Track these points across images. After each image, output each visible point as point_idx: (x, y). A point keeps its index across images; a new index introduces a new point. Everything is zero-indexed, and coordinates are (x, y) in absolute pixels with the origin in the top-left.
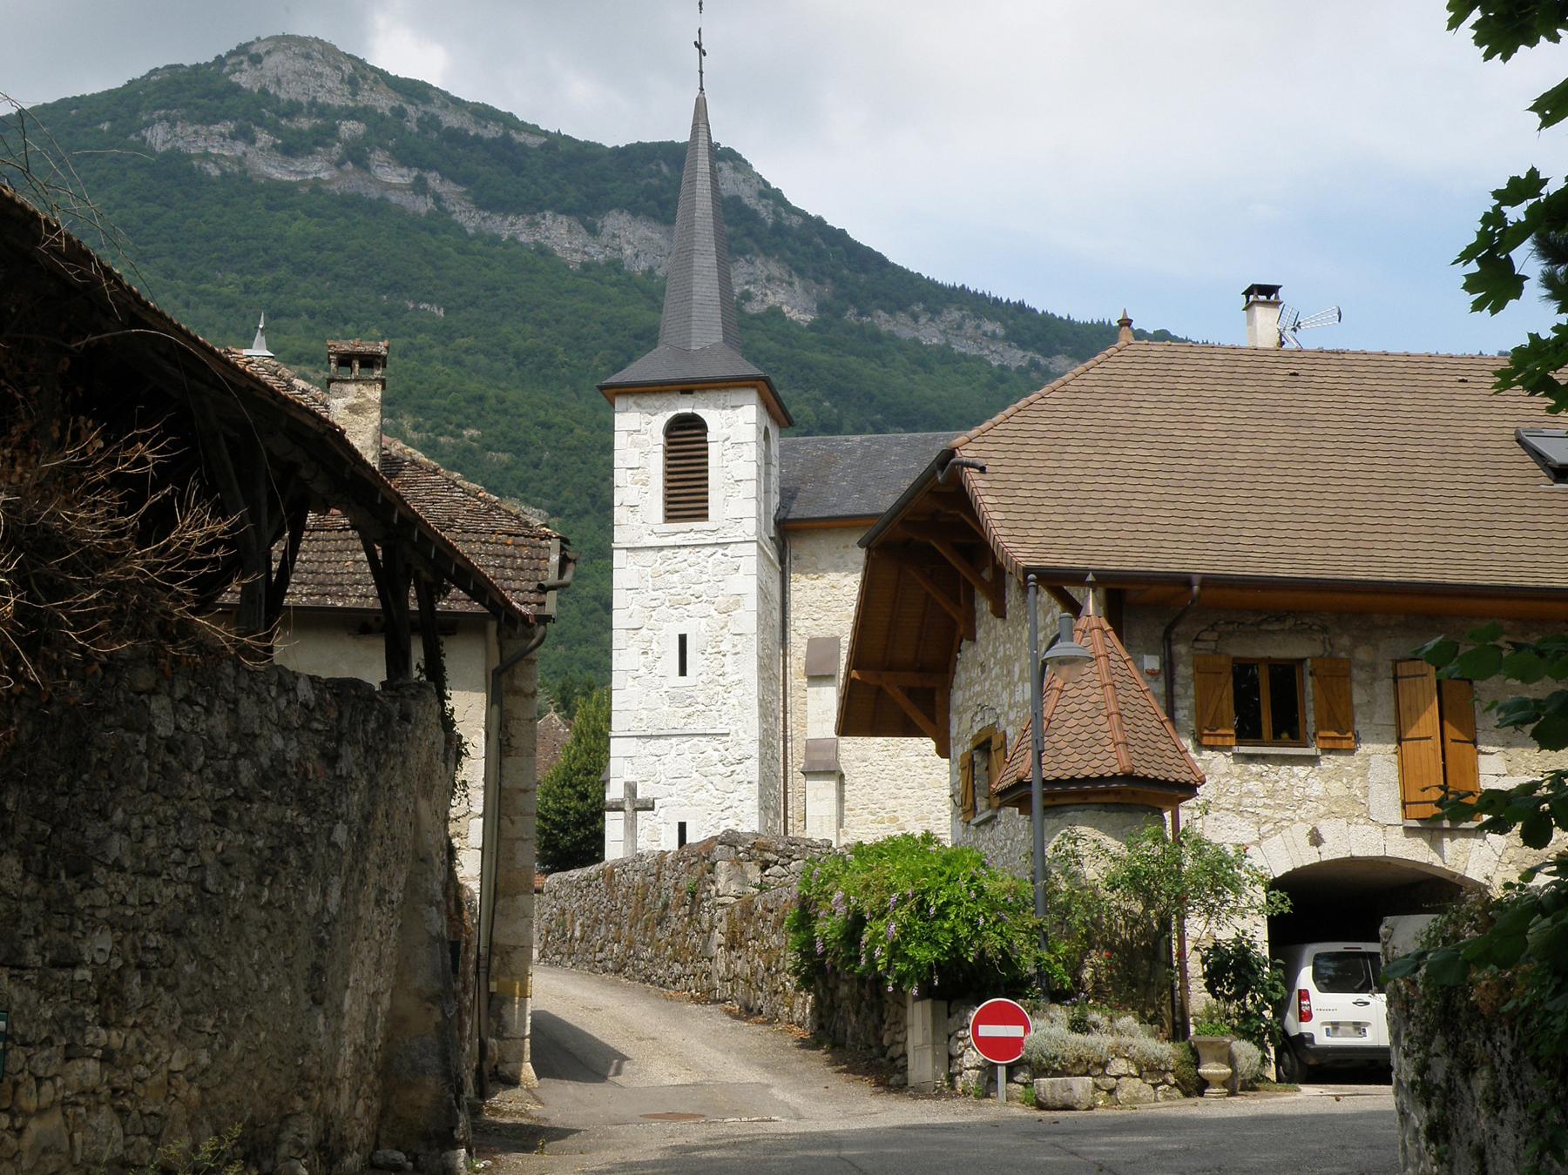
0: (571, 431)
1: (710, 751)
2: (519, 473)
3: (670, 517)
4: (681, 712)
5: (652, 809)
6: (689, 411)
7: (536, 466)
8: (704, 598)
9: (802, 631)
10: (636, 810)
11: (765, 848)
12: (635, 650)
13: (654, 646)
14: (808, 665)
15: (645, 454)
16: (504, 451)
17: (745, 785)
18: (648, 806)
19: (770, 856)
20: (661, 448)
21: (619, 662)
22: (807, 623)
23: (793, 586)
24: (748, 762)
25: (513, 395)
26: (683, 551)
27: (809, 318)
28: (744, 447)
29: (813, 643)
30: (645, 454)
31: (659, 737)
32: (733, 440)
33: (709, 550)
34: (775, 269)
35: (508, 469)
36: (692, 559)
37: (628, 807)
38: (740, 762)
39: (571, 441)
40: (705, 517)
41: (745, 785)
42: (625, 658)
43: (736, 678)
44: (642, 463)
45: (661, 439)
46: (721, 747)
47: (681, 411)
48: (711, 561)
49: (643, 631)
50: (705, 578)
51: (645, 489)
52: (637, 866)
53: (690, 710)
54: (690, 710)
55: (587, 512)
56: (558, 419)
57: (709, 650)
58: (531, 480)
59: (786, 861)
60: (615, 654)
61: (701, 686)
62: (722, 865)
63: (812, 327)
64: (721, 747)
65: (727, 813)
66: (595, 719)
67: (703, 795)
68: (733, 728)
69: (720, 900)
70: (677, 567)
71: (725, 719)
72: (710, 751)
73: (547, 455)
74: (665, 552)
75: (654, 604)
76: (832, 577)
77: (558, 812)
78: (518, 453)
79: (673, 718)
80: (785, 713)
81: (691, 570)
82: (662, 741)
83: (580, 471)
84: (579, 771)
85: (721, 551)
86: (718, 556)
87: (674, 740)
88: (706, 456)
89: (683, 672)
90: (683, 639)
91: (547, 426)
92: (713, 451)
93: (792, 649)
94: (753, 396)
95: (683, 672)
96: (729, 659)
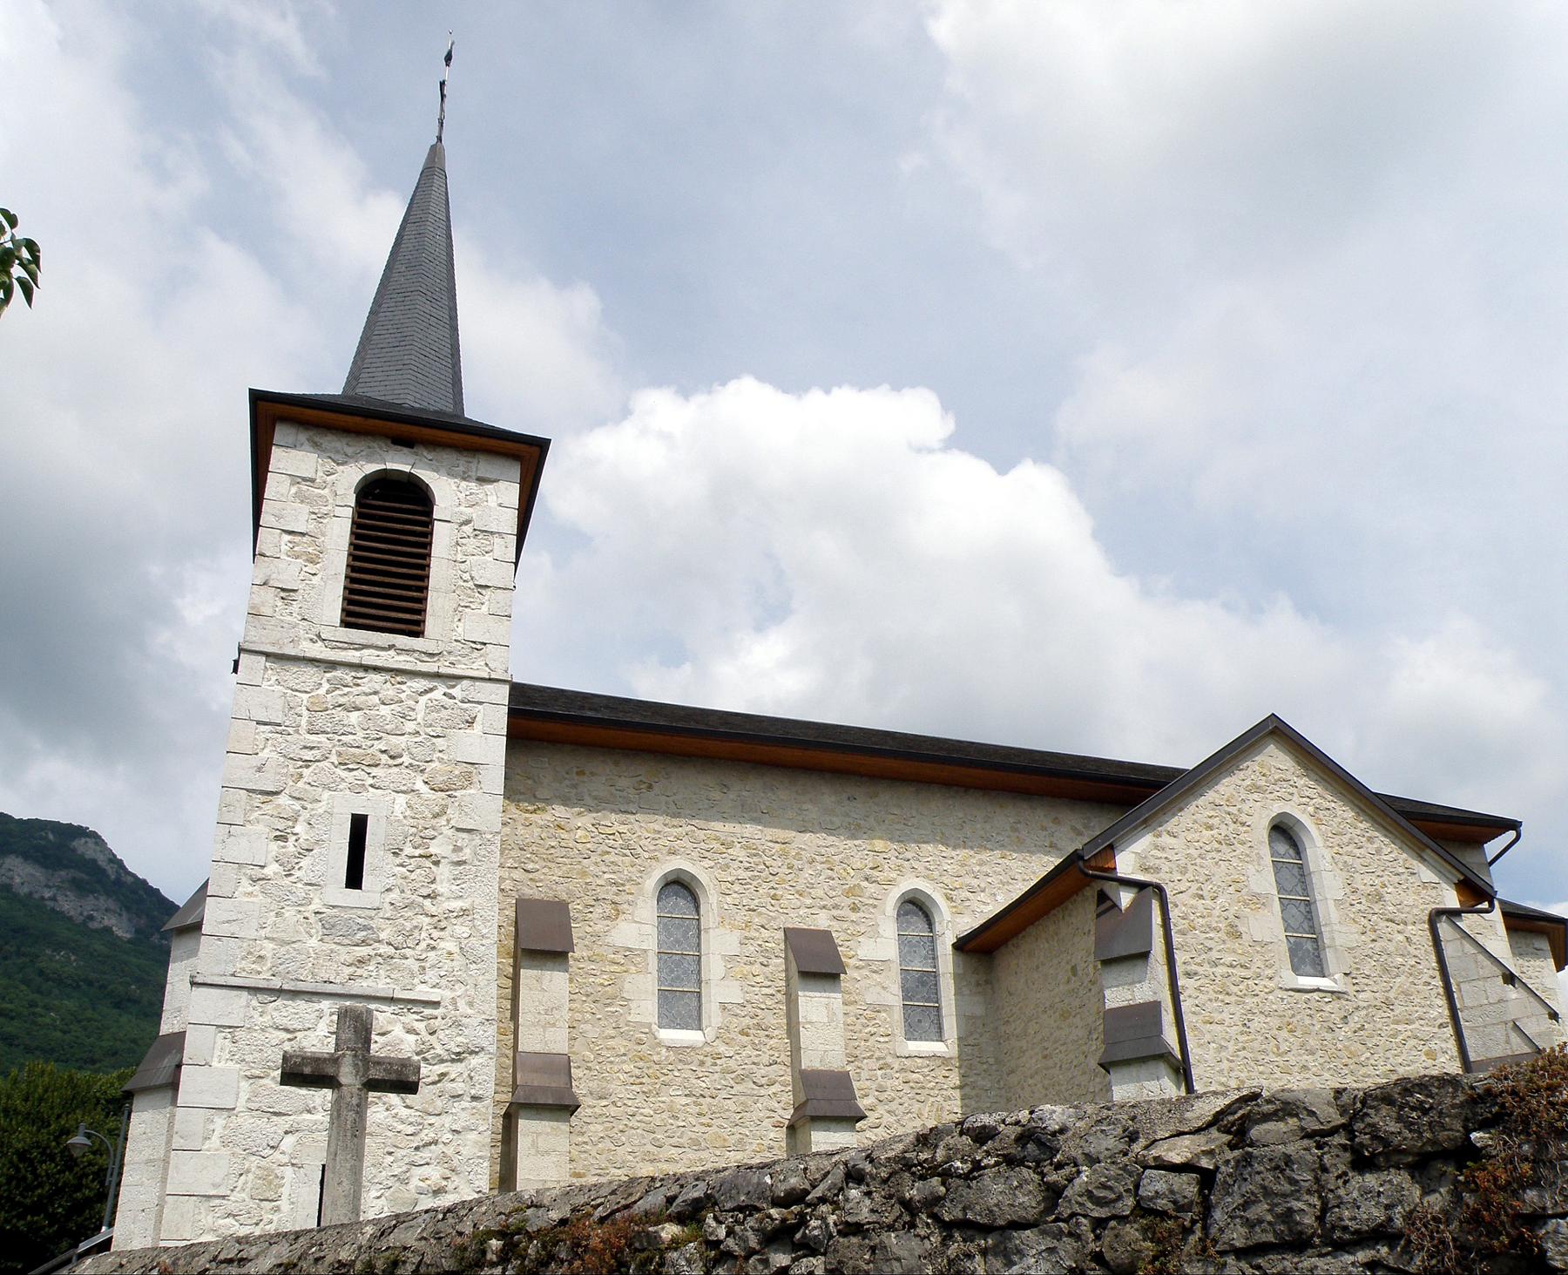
3: (346, 624)
4: (344, 954)
6: (407, 468)
8: (406, 759)
20: (349, 512)
24: (474, 1061)
26: (378, 677)
27: (128, 936)
28: (497, 540)
30: (320, 517)
31: (295, 994)
33: (421, 684)
34: (111, 904)
36: (389, 691)
37: (347, 1075)
38: (458, 1058)
40: (418, 634)
43: (457, 905)
44: (310, 527)
46: (421, 1026)
47: (390, 466)
48: (423, 702)
49: (283, 800)
50: (410, 727)
51: (311, 568)
53: (363, 951)
54: (363, 951)
57: (408, 850)
63: (129, 941)
64: (421, 1026)
65: (426, 1154)
68: (448, 994)
70: (359, 700)
71: (431, 976)
74: (338, 673)
75: (308, 755)
76: (560, 811)
81: (385, 710)
82: (301, 1004)
85: (442, 689)
86: (437, 694)
89: (354, 878)
90: (359, 826)
92: (442, 538)
94: (515, 471)
95: (354, 878)
96: (444, 871)
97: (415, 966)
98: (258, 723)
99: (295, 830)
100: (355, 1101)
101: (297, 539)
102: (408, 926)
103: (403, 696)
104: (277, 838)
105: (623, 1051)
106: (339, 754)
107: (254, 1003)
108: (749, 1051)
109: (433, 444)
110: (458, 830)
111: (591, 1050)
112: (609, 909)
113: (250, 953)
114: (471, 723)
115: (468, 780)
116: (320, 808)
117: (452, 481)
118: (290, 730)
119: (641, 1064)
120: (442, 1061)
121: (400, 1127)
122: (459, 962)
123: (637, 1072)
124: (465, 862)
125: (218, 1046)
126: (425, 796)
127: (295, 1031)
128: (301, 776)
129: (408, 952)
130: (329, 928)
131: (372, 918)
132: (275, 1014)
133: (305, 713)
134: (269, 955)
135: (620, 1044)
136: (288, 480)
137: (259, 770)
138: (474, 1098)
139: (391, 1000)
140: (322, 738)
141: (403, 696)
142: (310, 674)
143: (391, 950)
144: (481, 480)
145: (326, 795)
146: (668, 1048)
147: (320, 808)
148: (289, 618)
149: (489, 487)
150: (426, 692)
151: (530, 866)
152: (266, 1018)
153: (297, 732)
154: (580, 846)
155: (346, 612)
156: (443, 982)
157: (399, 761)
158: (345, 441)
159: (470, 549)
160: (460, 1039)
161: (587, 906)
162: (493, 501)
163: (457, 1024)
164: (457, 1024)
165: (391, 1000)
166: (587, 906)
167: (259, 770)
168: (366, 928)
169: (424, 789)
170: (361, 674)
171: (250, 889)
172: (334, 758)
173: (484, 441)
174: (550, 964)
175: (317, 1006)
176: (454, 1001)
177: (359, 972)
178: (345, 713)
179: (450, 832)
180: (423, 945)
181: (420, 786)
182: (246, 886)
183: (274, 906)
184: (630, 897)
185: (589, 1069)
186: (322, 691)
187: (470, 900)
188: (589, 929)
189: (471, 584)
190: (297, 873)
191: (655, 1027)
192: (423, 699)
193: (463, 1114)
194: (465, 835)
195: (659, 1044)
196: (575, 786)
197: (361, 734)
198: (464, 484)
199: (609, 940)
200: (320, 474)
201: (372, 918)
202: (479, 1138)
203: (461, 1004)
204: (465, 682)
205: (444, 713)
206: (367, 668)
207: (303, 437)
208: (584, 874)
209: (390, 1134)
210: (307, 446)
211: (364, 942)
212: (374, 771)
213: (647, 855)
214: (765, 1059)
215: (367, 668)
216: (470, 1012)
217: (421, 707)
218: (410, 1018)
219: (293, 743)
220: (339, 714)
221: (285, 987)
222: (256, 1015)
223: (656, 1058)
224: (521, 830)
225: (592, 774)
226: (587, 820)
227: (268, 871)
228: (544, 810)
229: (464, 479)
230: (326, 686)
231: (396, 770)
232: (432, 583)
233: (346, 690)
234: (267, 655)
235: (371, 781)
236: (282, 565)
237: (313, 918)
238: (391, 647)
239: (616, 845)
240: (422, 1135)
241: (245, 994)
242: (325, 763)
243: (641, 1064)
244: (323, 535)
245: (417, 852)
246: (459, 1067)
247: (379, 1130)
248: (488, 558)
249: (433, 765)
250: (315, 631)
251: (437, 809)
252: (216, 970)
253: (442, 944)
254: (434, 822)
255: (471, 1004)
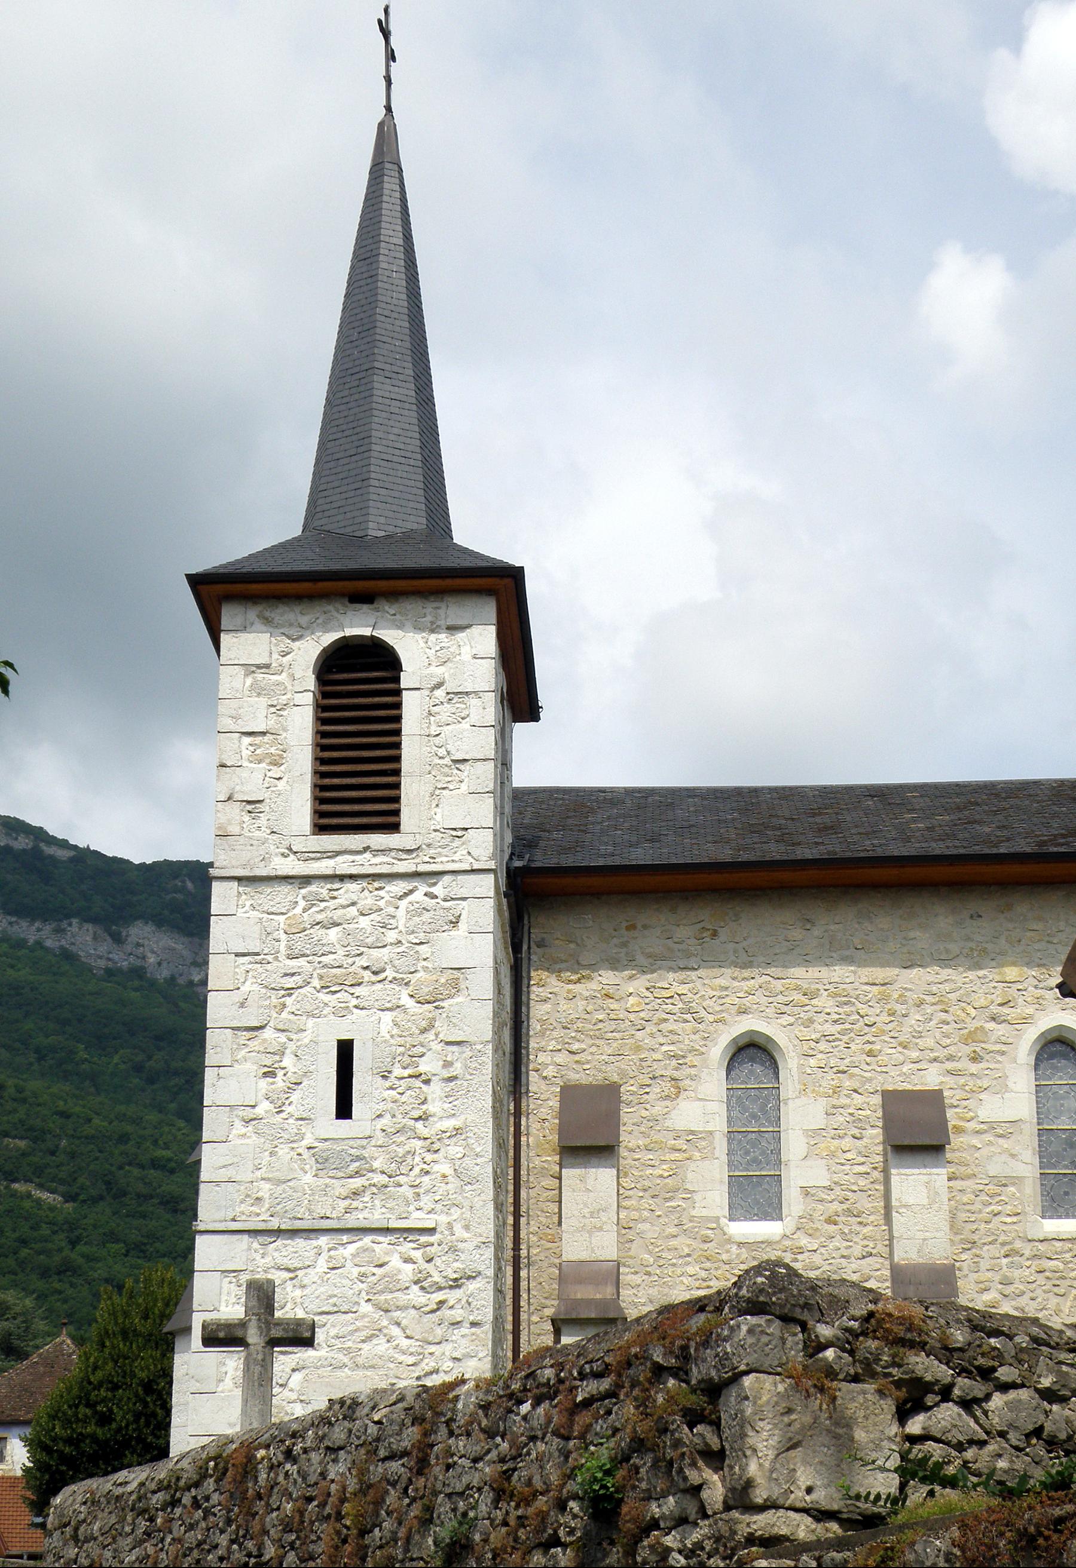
0: (90, 1120)
1: (395, 1262)
2: (35, 1159)
3: (320, 829)
4: (340, 1188)
5: (308, 1342)
6: (367, 632)
7: (53, 1153)
8: (389, 973)
9: (550, 1071)
10: (274, 1342)
11: (908, 1338)
12: (250, 1067)
13: (288, 1061)
14: (562, 1130)
15: (278, 709)
16: (21, 1138)
17: (465, 1330)
18: (301, 1337)
19: (928, 1367)
20: (309, 698)
21: (217, 1090)
22: (560, 1058)
23: (536, 992)
24: (471, 1286)
25: (34, 1085)
26: (353, 886)
28: (473, 701)
29: (570, 1093)
30: (278, 709)
31: (294, 1233)
32: (450, 686)
33: (399, 887)
35: (24, 1154)
36: (367, 900)
38: (456, 1284)
39: (88, 1130)
40: (394, 828)
41: (465, 1330)
42: (230, 1082)
43: (449, 1124)
44: (271, 723)
45: (311, 682)
46: (417, 1255)
47: (350, 632)
48: (406, 907)
49: (268, 1034)
50: (391, 936)
51: (276, 772)
52: (338, 1435)
53: (357, 1183)
54: (357, 1183)
55: (101, 1198)
56: (77, 1109)
57: (398, 1071)
58: (47, 1165)
59: (978, 1388)
60: (209, 1075)
61: (380, 1138)
62: (762, 1390)
64: (417, 1255)
66: (126, 1314)
67: (380, 1346)
68: (443, 1219)
69: (761, 1523)
70: (337, 915)
71: (426, 1201)
72: (395, 1262)
73: (64, 1143)
74: (313, 888)
75: (289, 982)
76: (607, 977)
77: (69, 1441)
78: (35, 1140)
79: (318, 1196)
80: (517, 1215)
81: (364, 922)
82: (300, 1243)
83: (97, 1159)
84: (100, 1384)
85: (423, 888)
86: (418, 896)
87: (323, 1241)
88: (398, 719)
89: (344, 1110)
90: (345, 1051)
91: (65, 1115)
92: (412, 707)
93: (530, 1104)
94: (489, 609)
95: (344, 1110)
96: (435, 1090)
97: (409, 1193)
98: (237, 955)
99: (283, 1065)
100: (260, 1357)
101: (258, 740)
102: (401, 1151)
103: (382, 903)
104: (266, 1075)
105: (686, 1251)
106: (321, 977)
107: (256, 1245)
108: (837, 1242)
109: (394, 595)
110: (448, 1043)
111: (650, 1253)
112: (667, 1087)
113: (248, 1196)
114: (455, 923)
115: (455, 987)
116: (306, 1038)
117: (418, 637)
118: (270, 958)
119: (708, 1265)
120: (440, 1289)
121: (402, 1358)
122: (454, 1184)
123: (704, 1274)
124: (455, 1078)
125: (225, 1291)
126: (411, 1011)
127: (296, 1270)
128: (284, 1006)
129: (402, 1179)
130: (322, 1162)
131: (364, 1147)
132: (276, 1254)
133: (283, 937)
134: (267, 1196)
135: (683, 1243)
136: (240, 671)
137: (242, 1005)
138: (474, 1324)
139: (387, 1231)
140: (302, 961)
141: (382, 903)
142: (284, 894)
143: (384, 1179)
144: (452, 629)
145: (311, 1022)
146: (740, 1244)
147: (306, 1038)
148: (257, 834)
149: (461, 636)
150: (406, 895)
151: (575, 1047)
152: (268, 1259)
153: (276, 959)
154: (632, 1017)
155: (318, 814)
156: (439, 1207)
157: (382, 976)
158: (297, 609)
159: (444, 718)
160: (456, 1265)
161: (642, 1086)
162: (466, 653)
163: (453, 1249)
164: (453, 1249)
165: (387, 1231)
166: (642, 1086)
167: (242, 1005)
168: (359, 1158)
169: (410, 1003)
170: (336, 886)
171: (244, 1130)
172: (316, 983)
173: (449, 582)
174: (594, 1160)
175: (315, 1243)
176: (450, 1226)
177: (355, 1204)
178: (323, 931)
179: (437, 1047)
180: (417, 1170)
181: (406, 1001)
182: (239, 1128)
183: (268, 1146)
184: (693, 1071)
185: (648, 1274)
186: (298, 910)
187: (463, 1117)
188: (645, 1113)
189: (447, 761)
190: (288, 1109)
191: (724, 1221)
192: (403, 904)
193: (464, 1342)
194: (455, 1048)
195: (729, 1241)
196: (624, 945)
197: (341, 952)
198: (433, 637)
199: (668, 1123)
200: (275, 656)
201: (364, 1147)
202: (480, 1364)
203: (458, 1229)
204: (447, 878)
205: (426, 916)
206: (342, 878)
207: (252, 613)
208: (638, 1049)
209: (392, 1365)
210: (258, 625)
211: (357, 1174)
212: (357, 991)
213: (711, 1018)
214: (857, 1251)
215: (342, 878)
216: (466, 1235)
217: (401, 913)
218: (407, 1248)
219: (273, 972)
220: (317, 932)
221: (283, 1227)
222: (258, 1257)
223: (725, 1257)
224: (564, 1006)
225: (645, 927)
226: (640, 984)
227: (259, 1111)
228: (589, 978)
229: (433, 631)
230: (302, 904)
231: (380, 986)
232: (406, 765)
233: (323, 905)
234: (239, 879)
235: (354, 1002)
236: (244, 774)
237: (306, 1155)
238: (366, 849)
239: (675, 1009)
240: (423, 1365)
241: (246, 1237)
242: (307, 989)
243: (708, 1265)
244: (285, 730)
245: (406, 1073)
246: (457, 1293)
247: (381, 1363)
248: (465, 725)
249: (417, 975)
250: (286, 843)
251: (424, 1024)
252: (220, 1215)
253: (436, 1168)
254: (421, 1038)
255: (467, 1228)
